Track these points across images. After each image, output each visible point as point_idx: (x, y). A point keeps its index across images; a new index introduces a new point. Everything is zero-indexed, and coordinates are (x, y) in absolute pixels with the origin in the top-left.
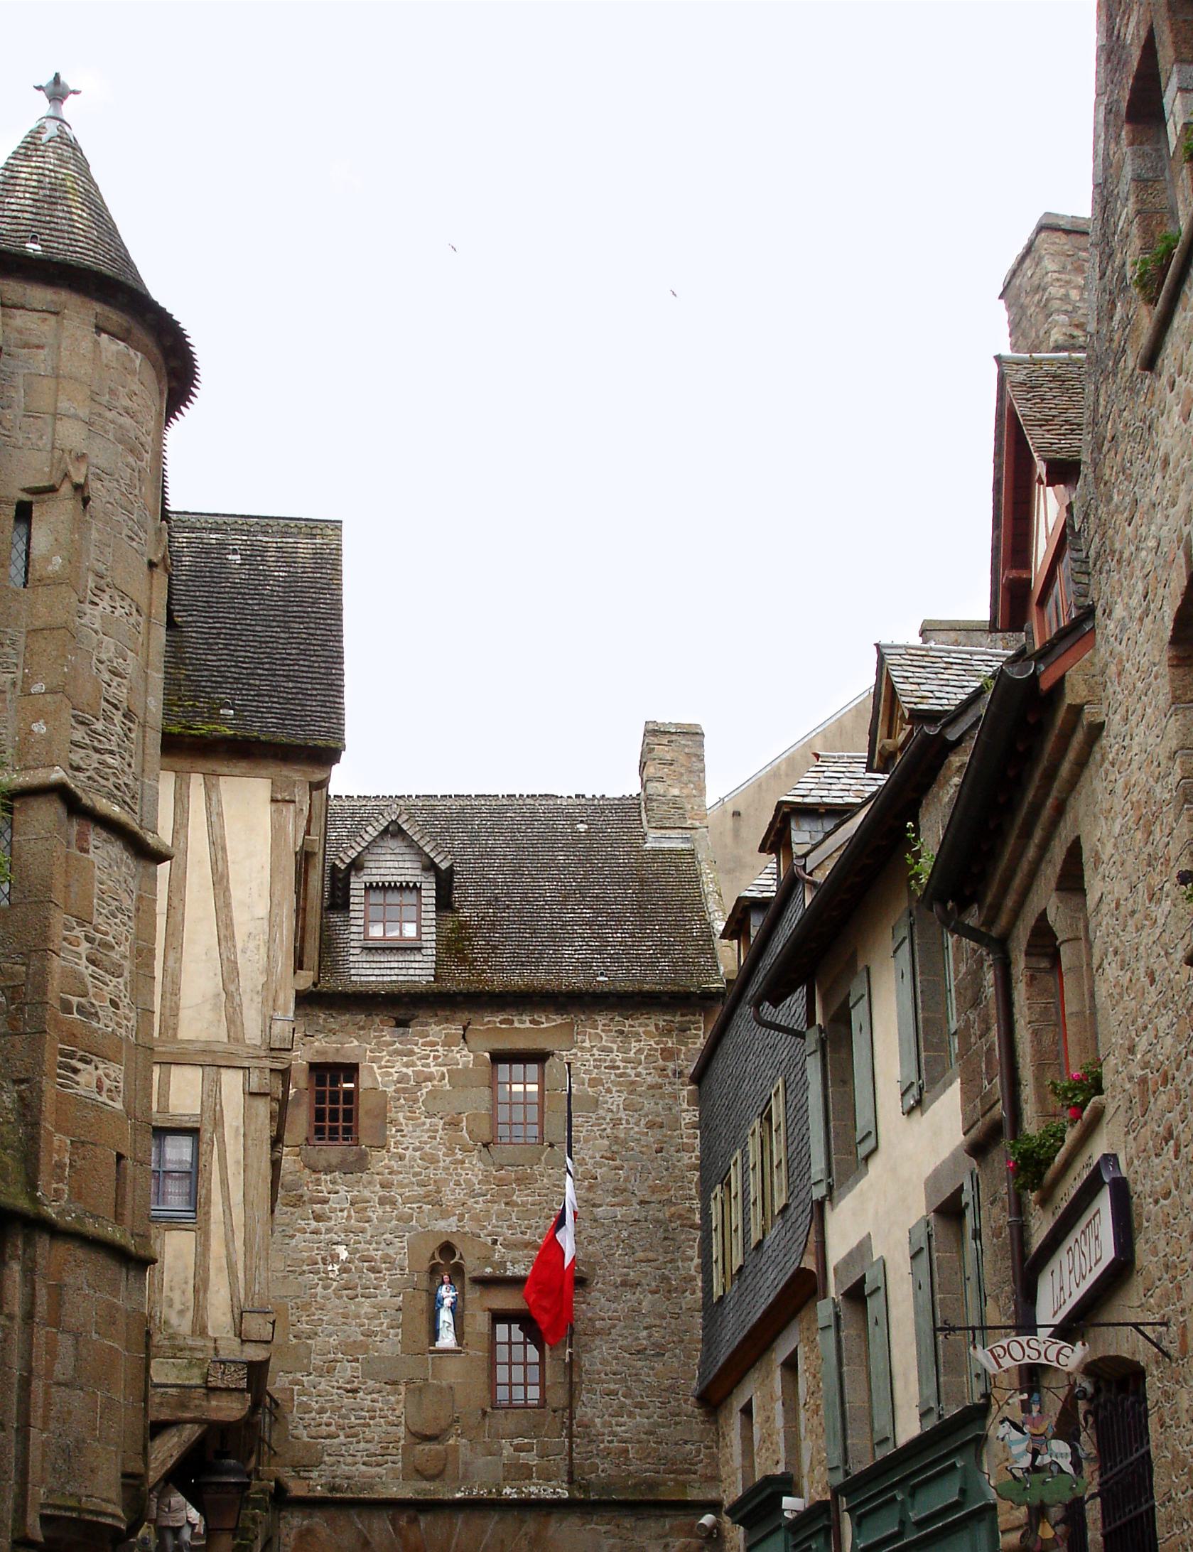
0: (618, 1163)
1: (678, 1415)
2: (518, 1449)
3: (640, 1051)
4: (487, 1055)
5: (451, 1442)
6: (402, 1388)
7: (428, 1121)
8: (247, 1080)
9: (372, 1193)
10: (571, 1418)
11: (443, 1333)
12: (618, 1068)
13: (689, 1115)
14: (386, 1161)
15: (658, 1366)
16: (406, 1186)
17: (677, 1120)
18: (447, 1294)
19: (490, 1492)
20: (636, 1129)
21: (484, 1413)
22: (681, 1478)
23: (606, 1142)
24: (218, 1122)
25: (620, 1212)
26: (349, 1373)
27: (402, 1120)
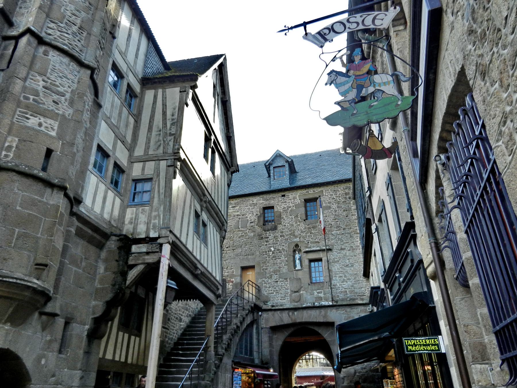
2: (318, 293)
5: (301, 292)
6: (288, 280)
9: (278, 234)
11: (297, 266)
15: (352, 269)
21: (309, 284)
22: (362, 297)
23: (333, 216)
25: (338, 232)
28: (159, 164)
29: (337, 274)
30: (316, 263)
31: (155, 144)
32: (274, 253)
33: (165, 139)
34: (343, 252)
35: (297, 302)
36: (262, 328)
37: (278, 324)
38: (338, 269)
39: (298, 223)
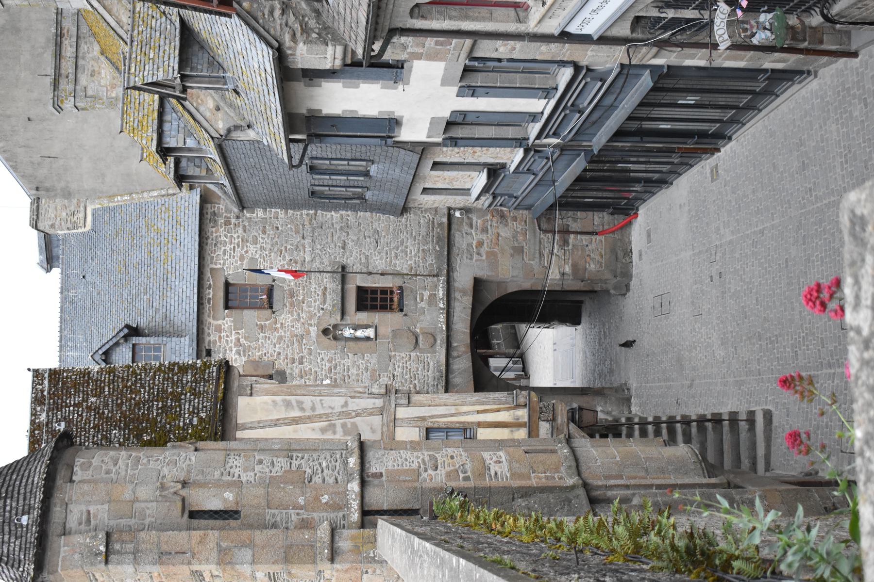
0: (283, 249)
1: (406, 225)
2: (422, 300)
3: (226, 236)
4: (226, 311)
5: (418, 331)
6: (393, 353)
7: (260, 341)
10: (407, 274)
11: (366, 334)
12: (234, 247)
13: (260, 213)
14: (281, 361)
16: (293, 351)
18: (348, 332)
19: (442, 313)
20: (266, 239)
21: (405, 315)
22: (436, 226)
23: (273, 254)
25: (308, 249)
27: (260, 353)
35: (435, 340)
39: (278, 325)
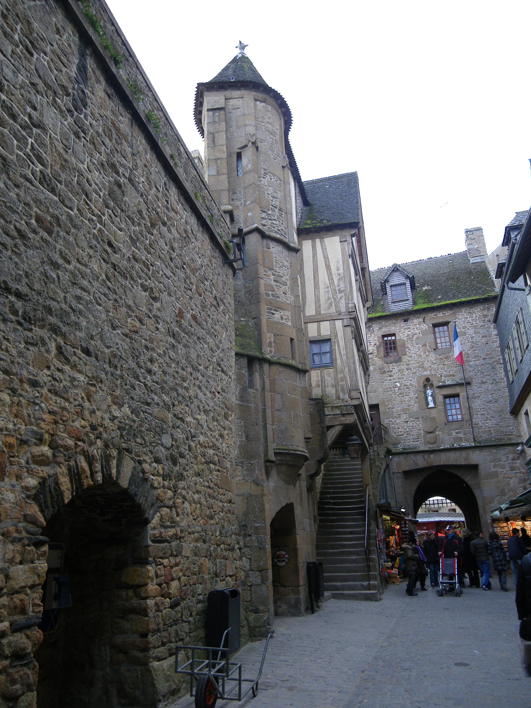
2: (457, 433)
6: (420, 420)
8: (343, 322)
9: (404, 367)
10: (472, 423)
11: (430, 403)
13: (495, 332)
15: (496, 405)
17: (491, 334)
18: (429, 392)
21: (446, 424)
22: (509, 437)
23: (470, 344)
24: (336, 336)
25: (477, 363)
26: (405, 417)
28: (334, 324)
29: (480, 411)
30: (452, 400)
31: (326, 303)
32: (400, 389)
33: (335, 297)
34: (484, 385)
35: (432, 444)
36: (393, 473)
37: (412, 468)
38: (479, 405)
39: (427, 354)
